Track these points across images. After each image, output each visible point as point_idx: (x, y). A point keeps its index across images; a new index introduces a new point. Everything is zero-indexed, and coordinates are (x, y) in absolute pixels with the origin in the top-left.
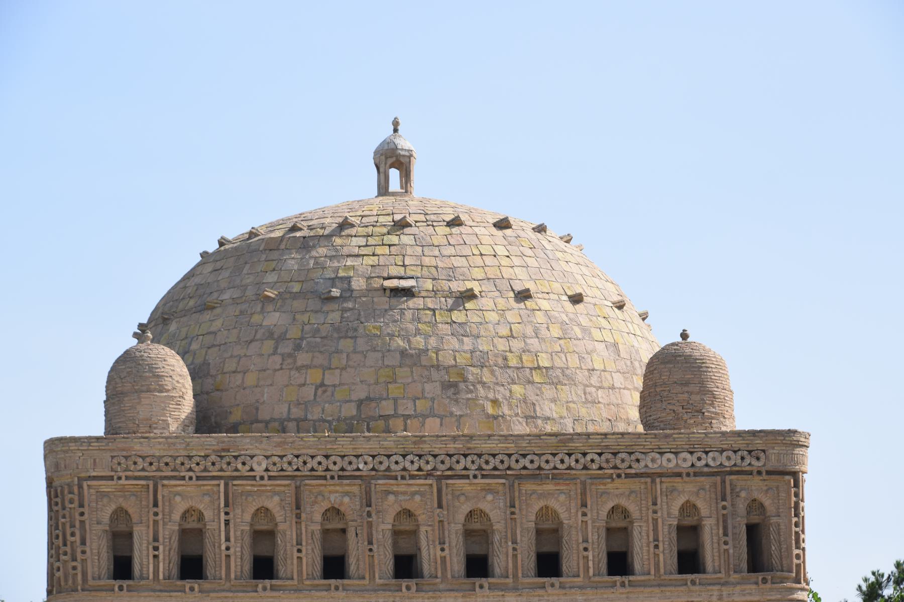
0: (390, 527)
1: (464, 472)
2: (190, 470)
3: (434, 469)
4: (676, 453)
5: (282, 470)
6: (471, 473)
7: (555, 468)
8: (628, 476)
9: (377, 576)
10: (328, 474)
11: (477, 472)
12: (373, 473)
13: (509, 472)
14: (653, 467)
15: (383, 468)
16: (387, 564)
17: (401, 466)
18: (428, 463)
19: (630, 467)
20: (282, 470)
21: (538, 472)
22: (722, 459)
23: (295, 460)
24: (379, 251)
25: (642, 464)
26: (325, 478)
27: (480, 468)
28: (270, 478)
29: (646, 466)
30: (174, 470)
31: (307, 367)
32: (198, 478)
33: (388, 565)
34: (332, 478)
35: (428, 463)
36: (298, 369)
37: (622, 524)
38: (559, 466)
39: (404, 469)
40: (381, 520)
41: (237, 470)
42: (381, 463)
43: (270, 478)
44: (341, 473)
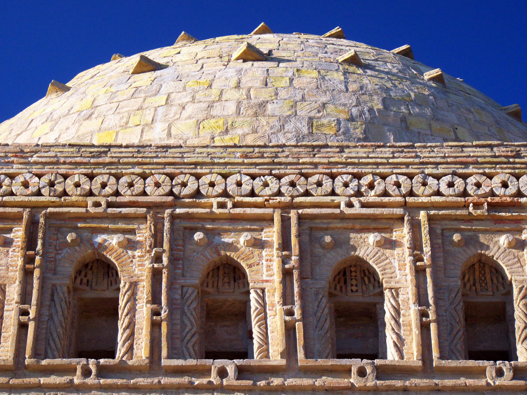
0: (197, 282)
3: (279, 193)
5: (12, 194)
6: (342, 201)
7: (492, 194)
9: (164, 352)
10: (90, 201)
11: (353, 199)
12: (170, 198)
13: (409, 199)
15: (186, 191)
16: (186, 340)
17: (219, 189)
18: (266, 185)
20: (12, 194)
23: (37, 179)
27: (358, 194)
33: (189, 341)
34: (97, 205)
35: (266, 185)
38: (499, 191)
39: (225, 194)
40: (179, 271)
42: (184, 185)
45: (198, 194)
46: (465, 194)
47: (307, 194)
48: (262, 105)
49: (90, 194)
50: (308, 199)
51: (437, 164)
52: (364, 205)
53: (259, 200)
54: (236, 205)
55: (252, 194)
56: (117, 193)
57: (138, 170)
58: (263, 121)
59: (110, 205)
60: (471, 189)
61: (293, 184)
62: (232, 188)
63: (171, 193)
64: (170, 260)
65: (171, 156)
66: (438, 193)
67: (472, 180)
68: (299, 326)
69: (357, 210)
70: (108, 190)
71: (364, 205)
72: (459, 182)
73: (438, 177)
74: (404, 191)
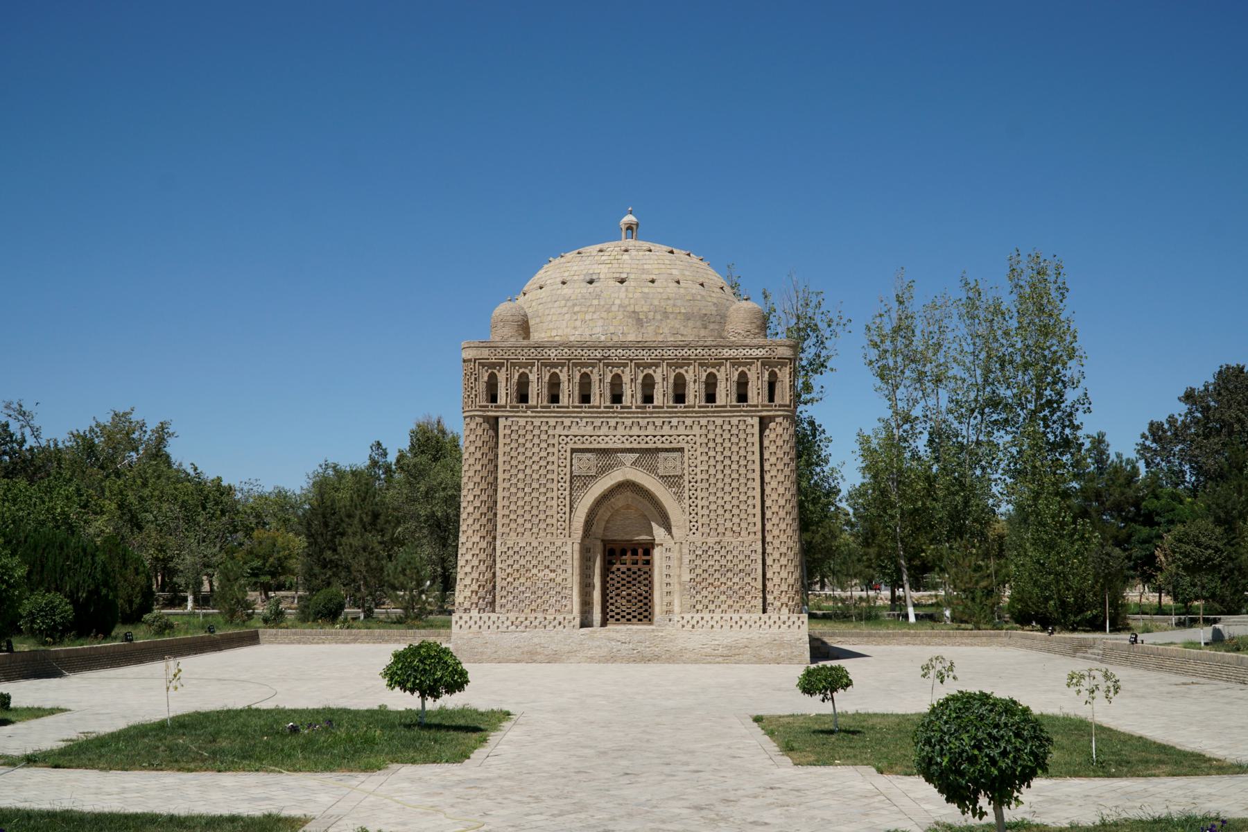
8: (715, 359)
14: (726, 355)
22: (757, 352)
24: (613, 262)
31: (578, 312)
36: (575, 313)
37: (713, 381)
69: (649, 361)
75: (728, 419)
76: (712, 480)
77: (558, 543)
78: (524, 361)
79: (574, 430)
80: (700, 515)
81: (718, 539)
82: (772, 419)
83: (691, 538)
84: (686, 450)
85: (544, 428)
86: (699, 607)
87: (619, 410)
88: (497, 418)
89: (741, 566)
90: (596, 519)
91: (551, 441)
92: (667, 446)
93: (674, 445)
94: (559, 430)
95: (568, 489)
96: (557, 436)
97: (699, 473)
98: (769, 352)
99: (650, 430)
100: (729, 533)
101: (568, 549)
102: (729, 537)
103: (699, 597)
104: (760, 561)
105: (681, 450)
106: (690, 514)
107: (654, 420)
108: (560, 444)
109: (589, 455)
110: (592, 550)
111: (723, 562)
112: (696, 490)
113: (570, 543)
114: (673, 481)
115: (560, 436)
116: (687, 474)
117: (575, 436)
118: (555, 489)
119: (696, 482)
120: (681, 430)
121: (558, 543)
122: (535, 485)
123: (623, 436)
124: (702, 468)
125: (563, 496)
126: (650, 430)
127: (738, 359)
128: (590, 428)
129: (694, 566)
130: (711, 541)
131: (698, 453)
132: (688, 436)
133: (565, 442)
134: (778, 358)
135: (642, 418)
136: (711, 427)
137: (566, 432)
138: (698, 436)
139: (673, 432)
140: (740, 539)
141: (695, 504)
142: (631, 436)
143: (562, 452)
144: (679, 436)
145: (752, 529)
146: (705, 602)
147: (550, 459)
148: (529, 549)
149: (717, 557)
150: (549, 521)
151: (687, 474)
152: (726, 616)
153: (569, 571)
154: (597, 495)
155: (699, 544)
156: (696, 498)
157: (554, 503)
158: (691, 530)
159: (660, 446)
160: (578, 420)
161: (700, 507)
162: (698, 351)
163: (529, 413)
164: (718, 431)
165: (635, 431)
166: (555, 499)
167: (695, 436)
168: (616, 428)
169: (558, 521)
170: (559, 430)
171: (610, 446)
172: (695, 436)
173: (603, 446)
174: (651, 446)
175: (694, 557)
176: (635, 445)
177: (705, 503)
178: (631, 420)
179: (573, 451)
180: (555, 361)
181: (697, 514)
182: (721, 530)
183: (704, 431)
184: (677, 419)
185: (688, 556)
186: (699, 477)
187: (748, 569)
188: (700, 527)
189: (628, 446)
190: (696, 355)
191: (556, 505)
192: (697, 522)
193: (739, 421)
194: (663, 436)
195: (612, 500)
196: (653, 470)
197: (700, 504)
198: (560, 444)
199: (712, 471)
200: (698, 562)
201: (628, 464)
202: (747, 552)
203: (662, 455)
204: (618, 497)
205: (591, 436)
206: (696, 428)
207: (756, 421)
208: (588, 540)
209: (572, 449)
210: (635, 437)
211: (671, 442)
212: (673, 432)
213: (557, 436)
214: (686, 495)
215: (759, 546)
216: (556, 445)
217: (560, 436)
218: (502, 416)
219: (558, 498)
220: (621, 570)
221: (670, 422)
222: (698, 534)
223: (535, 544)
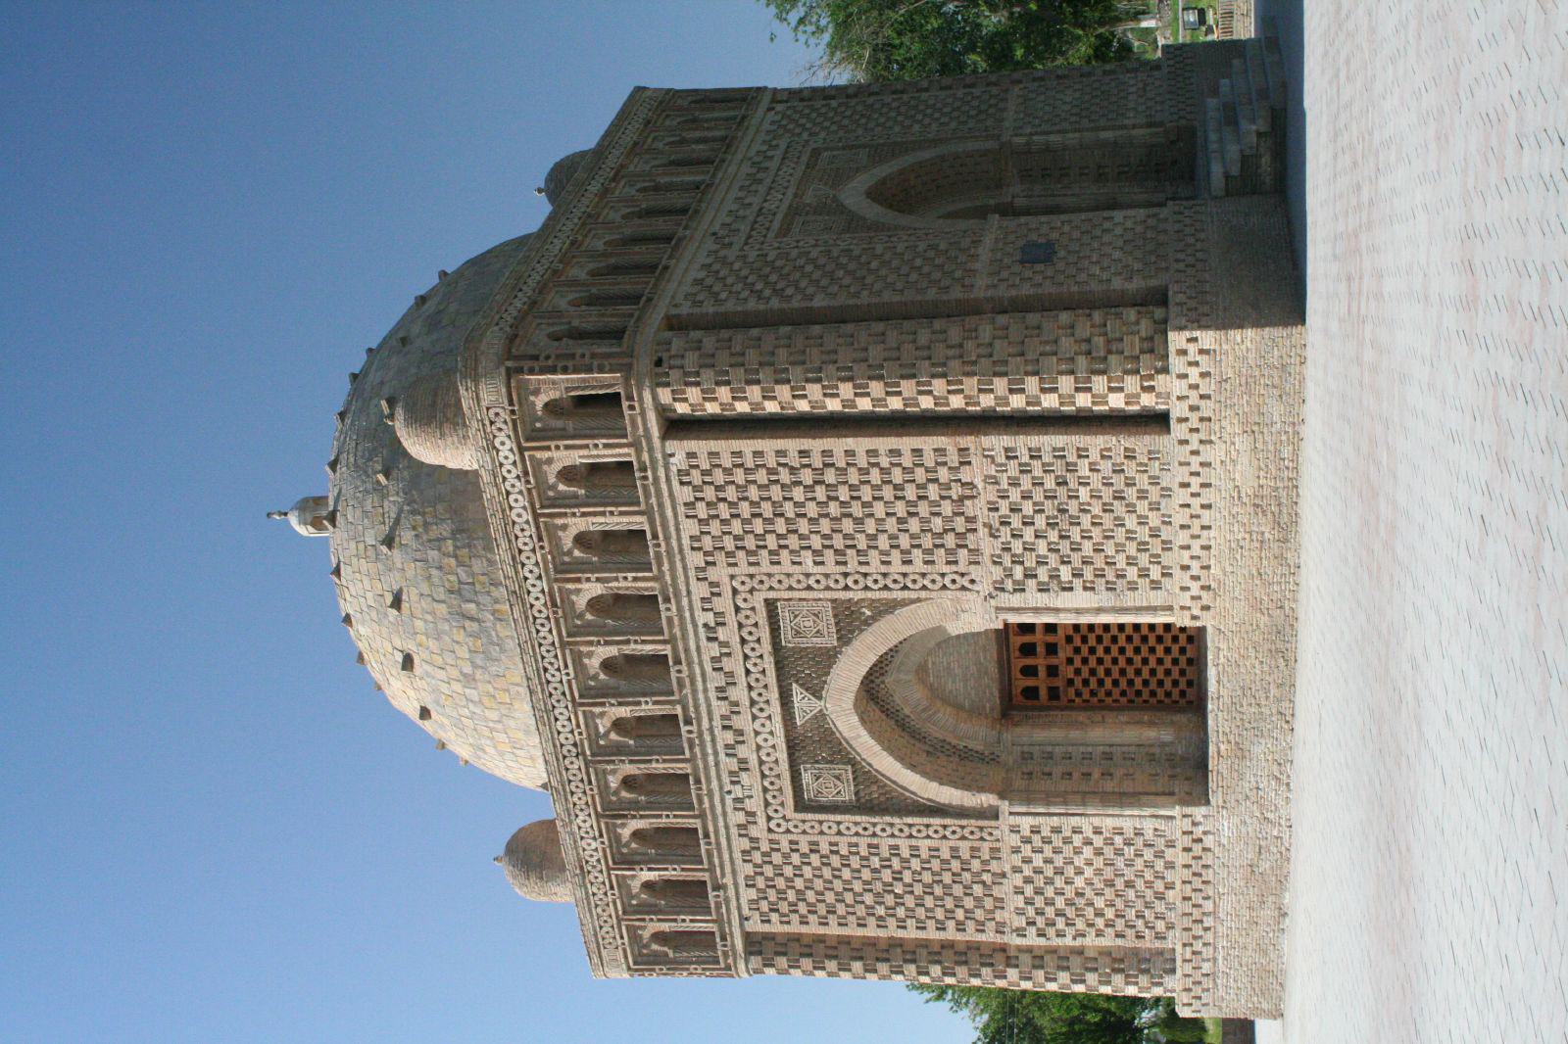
1: (566, 685)
2: (606, 894)
4: (508, 493)
7: (545, 604)
8: (540, 539)
19: (531, 536)
21: (552, 621)
22: (504, 451)
25: (526, 527)
26: (593, 796)
28: (601, 836)
29: (527, 522)
30: (608, 905)
32: (612, 888)
39: (572, 732)
41: (599, 861)
43: (601, 836)
44: (586, 782)
45: (575, 745)
46: (548, 618)
47: (564, 694)
48: (465, 675)
49: (585, 792)
50: (567, 693)
51: (529, 632)
52: (566, 667)
53: (572, 717)
54: (578, 726)
55: (569, 719)
56: (582, 781)
57: (564, 772)
58: (478, 677)
59: (590, 783)
60: (543, 615)
61: (558, 701)
62: (567, 729)
63: (577, 756)
64: (621, 755)
65: (552, 759)
66: (550, 631)
67: (537, 615)
68: (654, 699)
69: (571, 670)
70: (580, 785)
71: (566, 667)
72: (538, 621)
73: (538, 631)
74: (552, 648)
75: (681, 510)
76: (838, 542)
77: (1014, 840)
78: (616, 892)
79: (755, 804)
80: (925, 569)
81: (983, 532)
82: (663, 411)
83: (985, 587)
84: (772, 595)
85: (757, 857)
86: (1155, 573)
87: (694, 728)
88: (748, 937)
89: (1050, 483)
90: (954, 742)
91: (785, 846)
92: (765, 634)
93: (762, 617)
94: (758, 830)
95: (888, 819)
96: (772, 836)
97: (820, 569)
98: (500, 425)
99: (734, 664)
100: (969, 507)
101: (1026, 823)
102: (977, 508)
103: (1132, 573)
104: (1035, 440)
105: (771, 605)
106: (924, 588)
107: (706, 658)
108: (788, 831)
109: (807, 778)
110: (1026, 749)
111: (1040, 522)
112: (865, 575)
113: (1013, 820)
114: (849, 621)
115: (770, 830)
116: (829, 595)
117: (767, 804)
118: (892, 841)
119: (846, 575)
120: (724, 604)
121: (1014, 840)
122: (887, 875)
123: (754, 718)
124: (811, 564)
125: (906, 829)
126: (734, 664)
127: (529, 490)
128: (744, 777)
129: (1054, 585)
130: (988, 546)
131: (775, 569)
132: (735, 592)
133: (781, 821)
134: (511, 403)
135: (704, 681)
136: (707, 543)
137: (761, 820)
138: (731, 570)
139: (731, 619)
140: (979, 482)
141: (900, 578)
142: (753, 703)
143: (807, 826)
144: (737, 609)
145: (953, 459)
146: (1144, 559)
147: (825, 848)
148: (1029, 890)
149: (1029, 534)
150: (965, 854)
151: (829, 595)
152: (1180, 517)
153: (1075, 821)
154: (898, 765)
155: (997, 572)
156: (885, 575)
157: (924, 845)
158: (963, 588)
159: (766, 647)
160: (729, 799)
161: (906, 569)
162: (528, 575)
163: (728, 880)
164: (715, 527)
165: (738, 693)
166: (914, 842)
167: (732, 577)
168: (740, 732)
169: (963, 838)
170: (758, 830)
171: (780, 741)
172: (732, 577)
173: (782, 755)
174: (769, 664)
175: (1031, 583)
176: (774, 695)
177: (896, 557)
178: (715, 703)
179: (801, 805)
180: (605, 839)
181: (924, 575)
182: (960, 524)
183: (720, 557)
184: (698, 613)
185: (1028, 594)
186: (831, 567)
187: (1059, 467)
188: (954, 568)
189: (775, 708)
190: (540, 578)
191: (928, 842)
192: (943, 575)
193: (682, 483)
194: (743, 641)
195: (907, 711)
196: (826, 659)
197: (897, 567)
198: (788, 831)
199: (816, 542)
200: (1043, 574)
201: (818, 705)
202: (1013, 468)
203: (787, 639)
204: (897, 699)
205: (763, 776)
206: (713, 574)
207: (679, 450)
208: (1003, 757)
209: (796, 810)
210: (754, 694)
211: (756, 625)
212: (731, 619)
213: (772, 836)
214: (885, 595)
215: (997, 442)
216: (791, 837)
217: (770, 830)
218: (741, 925)
219: (911, 836)
220: (1071, 675)
221: (705, 625)
222: (975, 572)
223: (1018, 879)
